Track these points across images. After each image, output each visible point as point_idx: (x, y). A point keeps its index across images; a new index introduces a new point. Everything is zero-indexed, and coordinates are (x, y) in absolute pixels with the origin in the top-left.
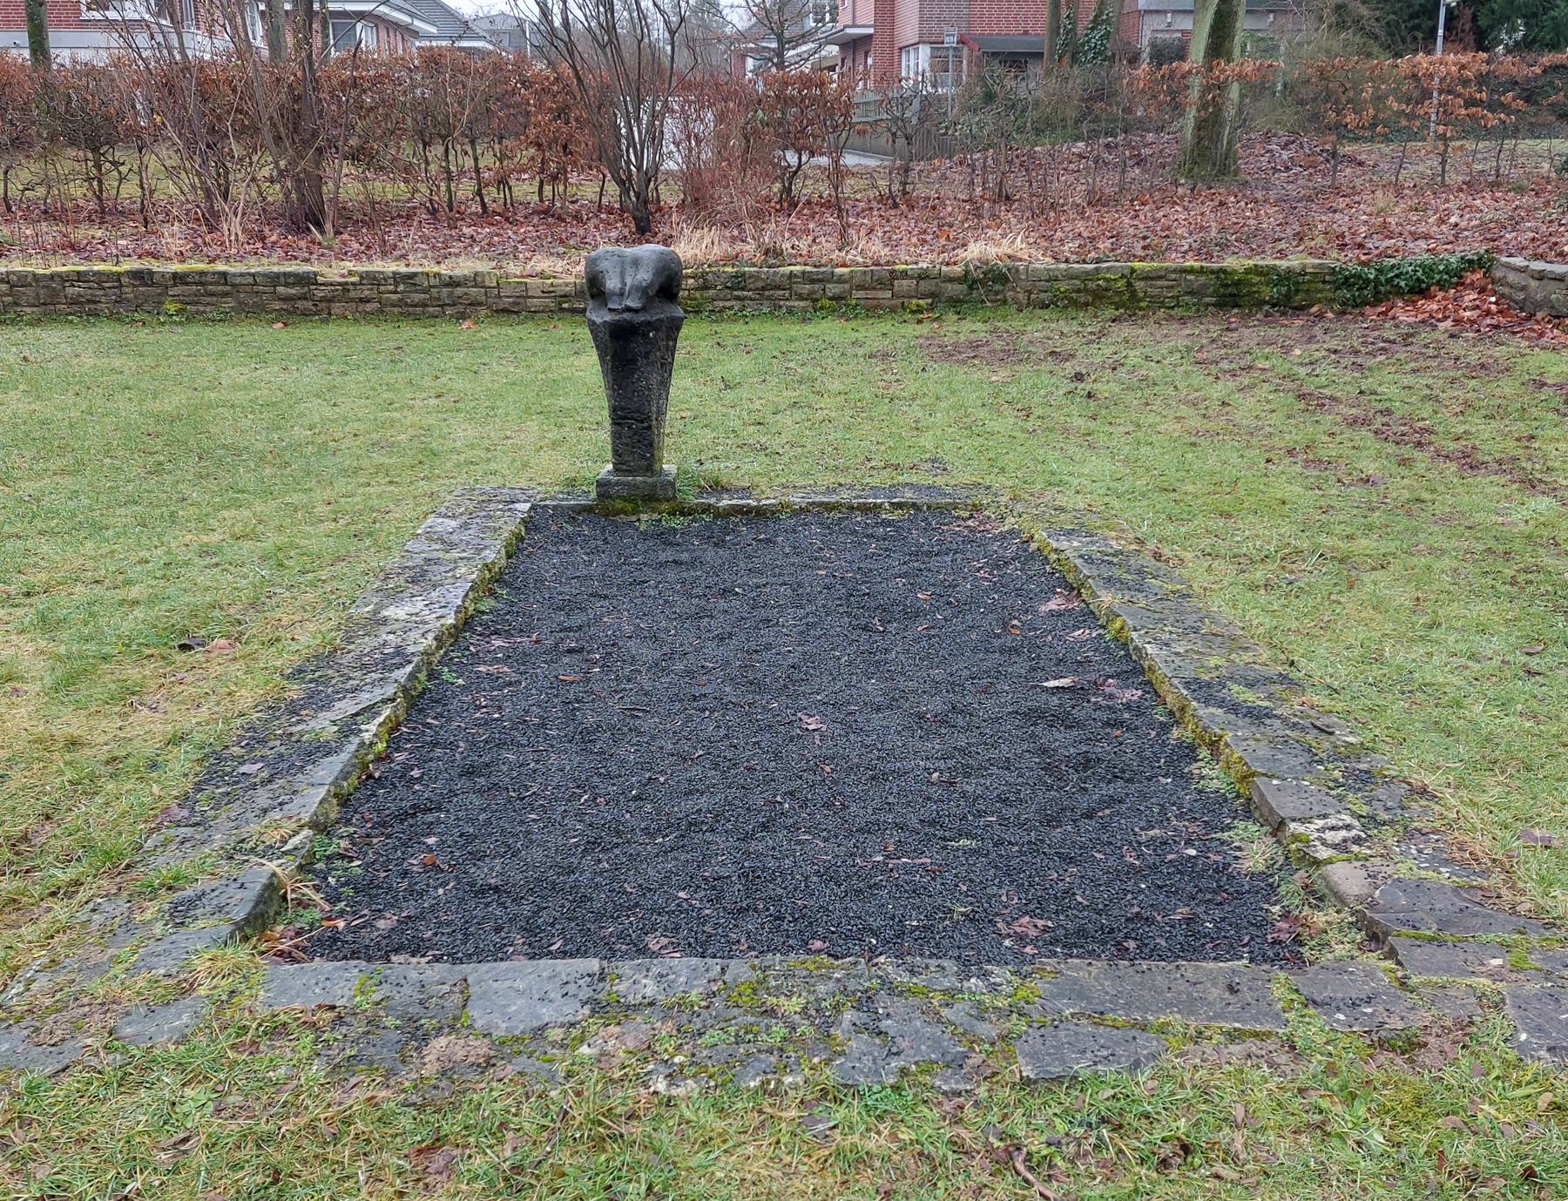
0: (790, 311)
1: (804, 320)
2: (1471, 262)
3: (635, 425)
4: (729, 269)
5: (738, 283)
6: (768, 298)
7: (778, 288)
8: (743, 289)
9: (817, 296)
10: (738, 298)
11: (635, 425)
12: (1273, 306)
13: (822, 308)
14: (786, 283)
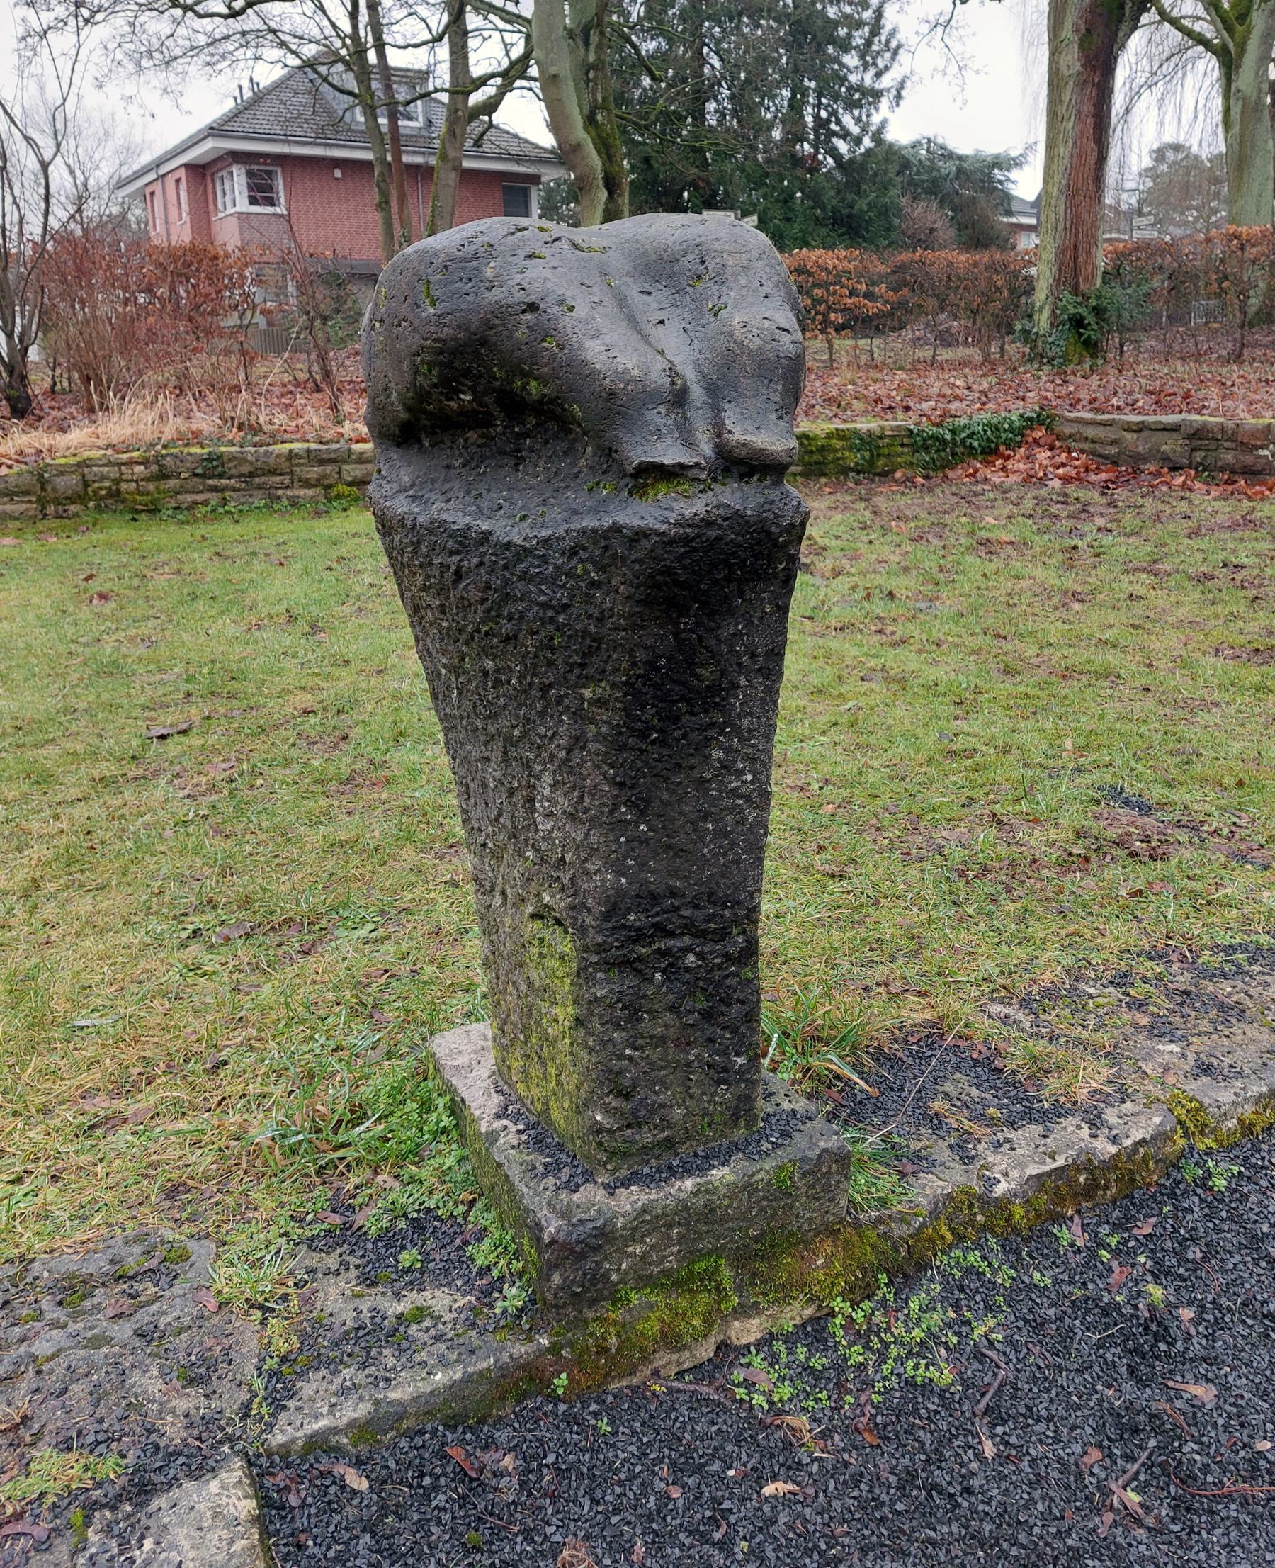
0: (294, 503)
1: (318, 514)
2: (1030, 419)
3: (671, 954)
4: (196, 450)
5: (213, 467)
6: (259, 487)
7: (273, 472)
8: (221, 476)
9: (332, 481)
10: (214, 489)
11: (671, 954)
12: (858, 472)
13: (339, 497)
14: (285, 466)
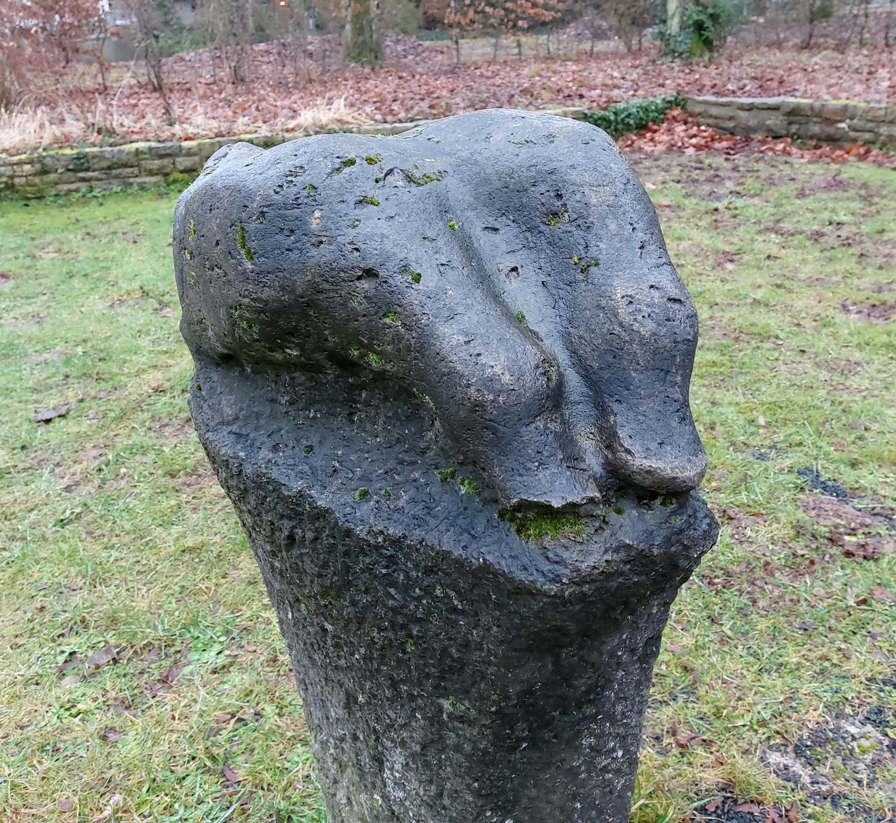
0: (143, 188)
1: (161, 196)
2: (670, 102)
4: (68, 151)
5: (81, 164)
6: (117, 177)
7: (126, 165)
8: (87, 170)
10: (83, 180)
14: (134, 160)
